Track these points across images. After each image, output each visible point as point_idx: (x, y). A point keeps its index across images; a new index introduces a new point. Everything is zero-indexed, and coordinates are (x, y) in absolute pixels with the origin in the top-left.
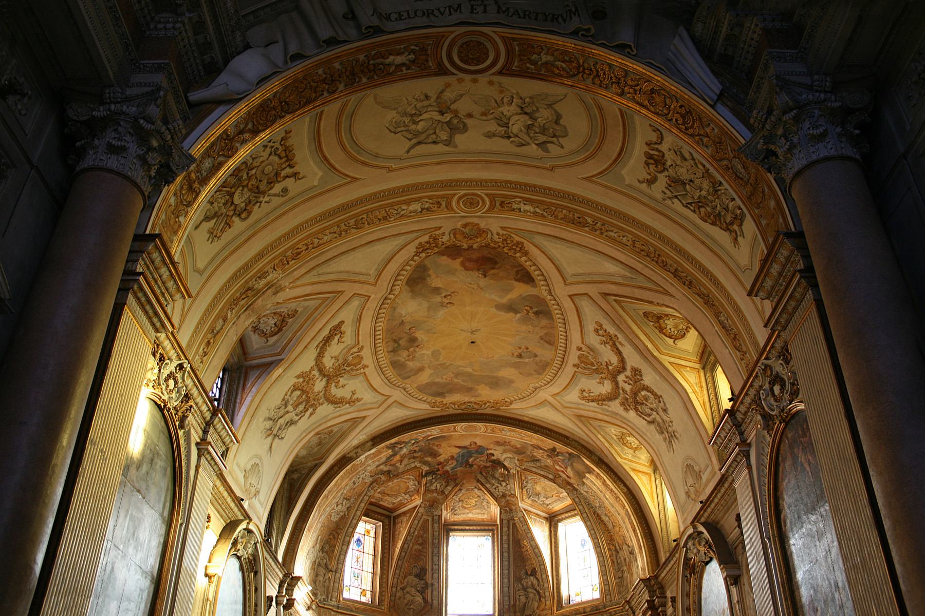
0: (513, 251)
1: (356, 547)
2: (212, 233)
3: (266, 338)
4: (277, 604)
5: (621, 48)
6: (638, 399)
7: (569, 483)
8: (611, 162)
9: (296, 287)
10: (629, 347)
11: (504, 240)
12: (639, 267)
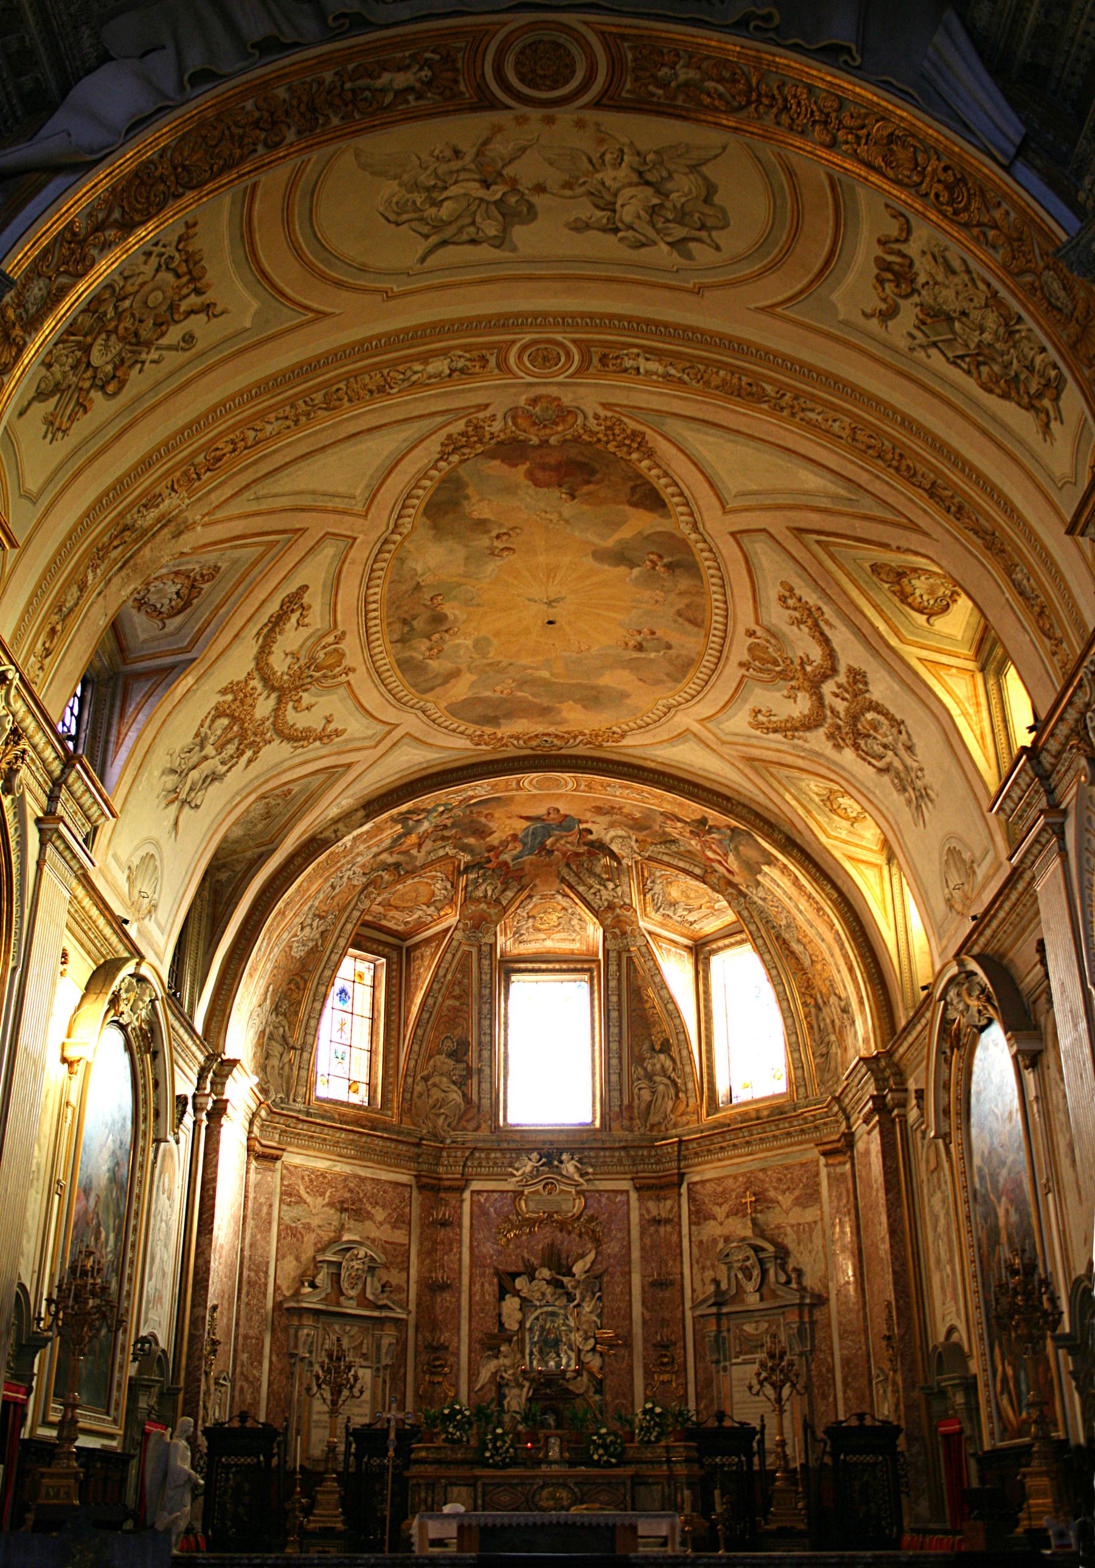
0: (625, 449)
1: (338, 1004)
2: (52, 423)
3: (162, 620)
4: (196, 1109)
6: (859, 726)
7: (730, 884)
8: (811, 276)
9: (216, 523)
10: (844, 629)
11: (608, 428)
12: (863, 478)
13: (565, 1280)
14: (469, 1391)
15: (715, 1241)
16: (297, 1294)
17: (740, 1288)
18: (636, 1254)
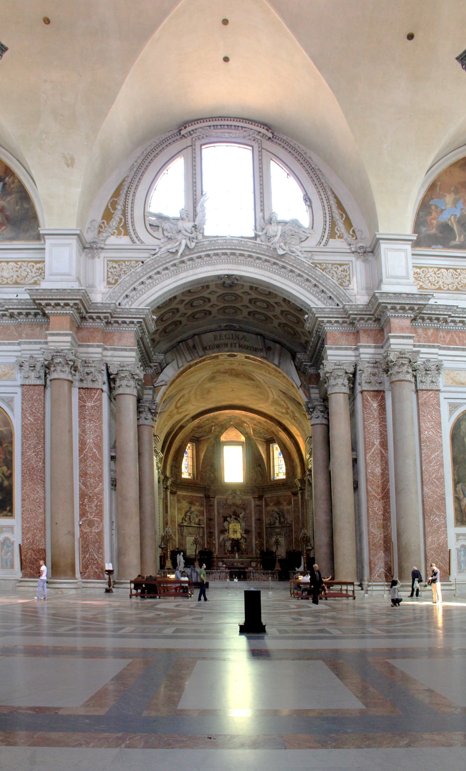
5: (275, 365)
15: (270, 511)
18: (253, 513)
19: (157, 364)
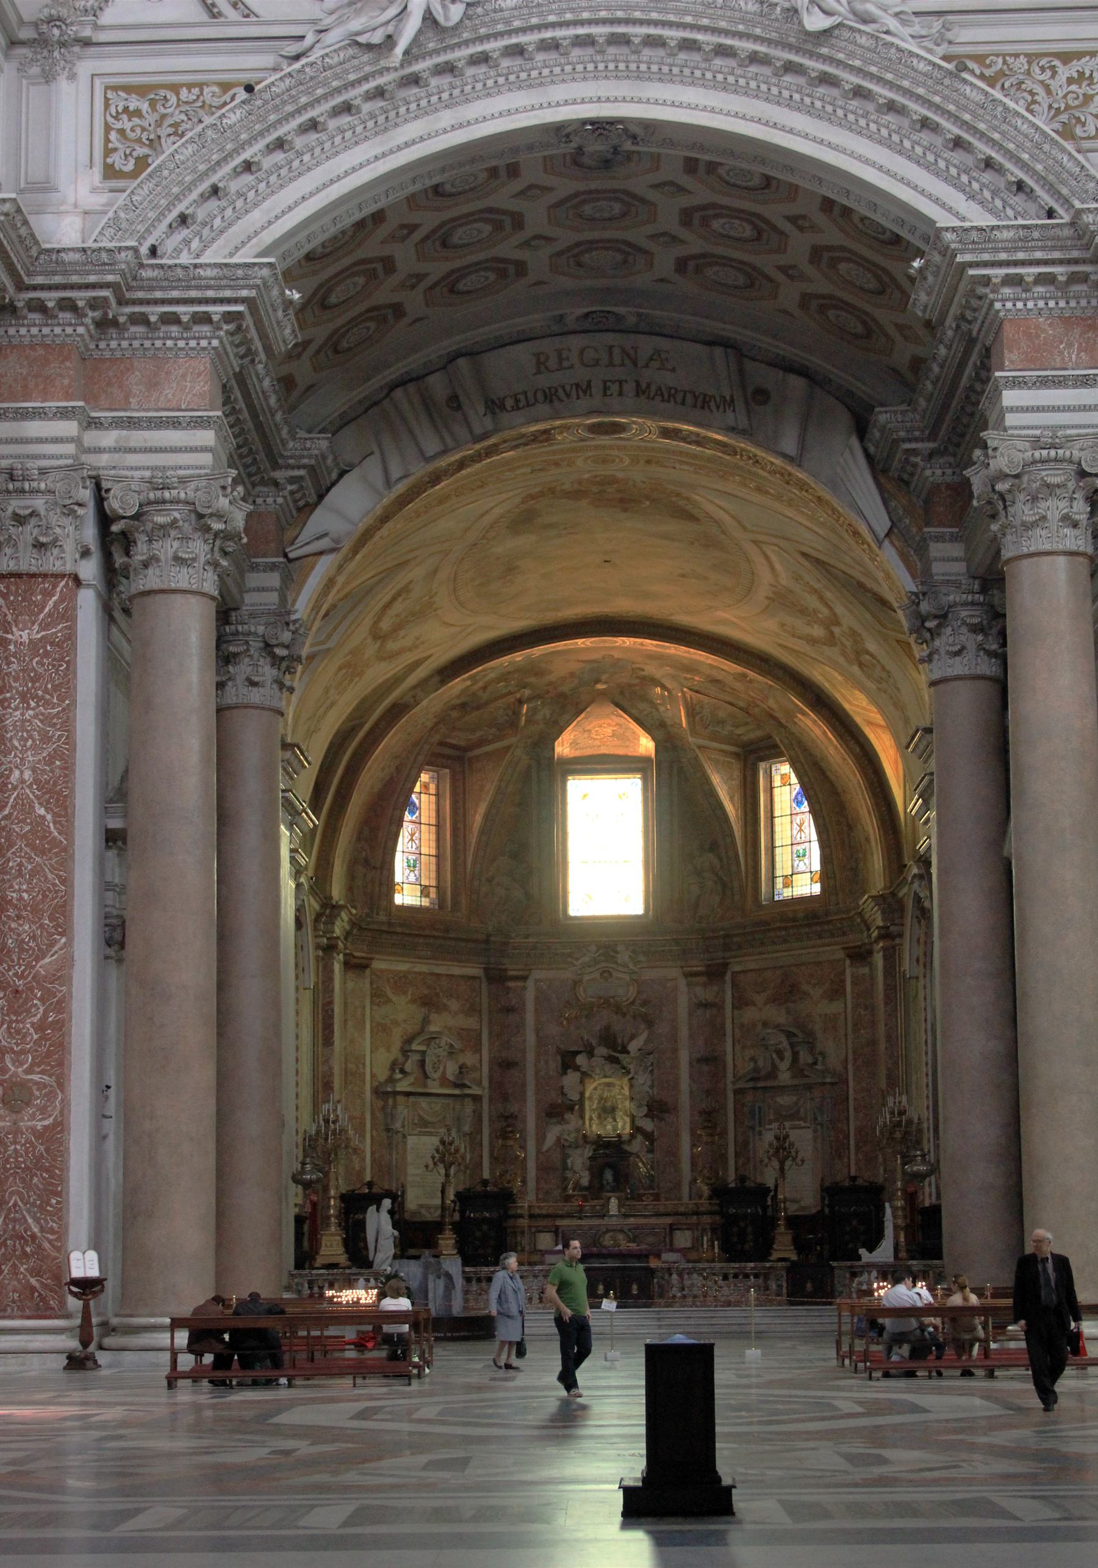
13: (621, 1056)
14: (539, 1152)
16: (391, 1080)
17: (774, 1066)
18: (684, 1033)
19: (302, 472)
